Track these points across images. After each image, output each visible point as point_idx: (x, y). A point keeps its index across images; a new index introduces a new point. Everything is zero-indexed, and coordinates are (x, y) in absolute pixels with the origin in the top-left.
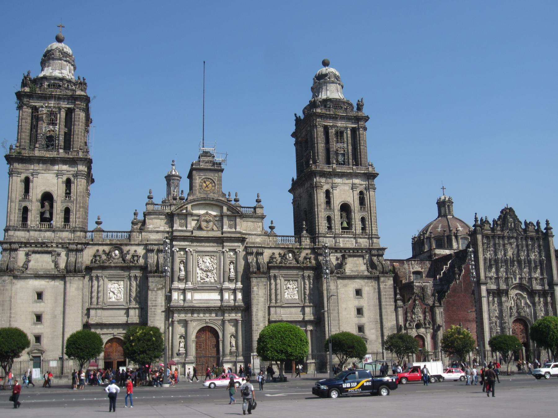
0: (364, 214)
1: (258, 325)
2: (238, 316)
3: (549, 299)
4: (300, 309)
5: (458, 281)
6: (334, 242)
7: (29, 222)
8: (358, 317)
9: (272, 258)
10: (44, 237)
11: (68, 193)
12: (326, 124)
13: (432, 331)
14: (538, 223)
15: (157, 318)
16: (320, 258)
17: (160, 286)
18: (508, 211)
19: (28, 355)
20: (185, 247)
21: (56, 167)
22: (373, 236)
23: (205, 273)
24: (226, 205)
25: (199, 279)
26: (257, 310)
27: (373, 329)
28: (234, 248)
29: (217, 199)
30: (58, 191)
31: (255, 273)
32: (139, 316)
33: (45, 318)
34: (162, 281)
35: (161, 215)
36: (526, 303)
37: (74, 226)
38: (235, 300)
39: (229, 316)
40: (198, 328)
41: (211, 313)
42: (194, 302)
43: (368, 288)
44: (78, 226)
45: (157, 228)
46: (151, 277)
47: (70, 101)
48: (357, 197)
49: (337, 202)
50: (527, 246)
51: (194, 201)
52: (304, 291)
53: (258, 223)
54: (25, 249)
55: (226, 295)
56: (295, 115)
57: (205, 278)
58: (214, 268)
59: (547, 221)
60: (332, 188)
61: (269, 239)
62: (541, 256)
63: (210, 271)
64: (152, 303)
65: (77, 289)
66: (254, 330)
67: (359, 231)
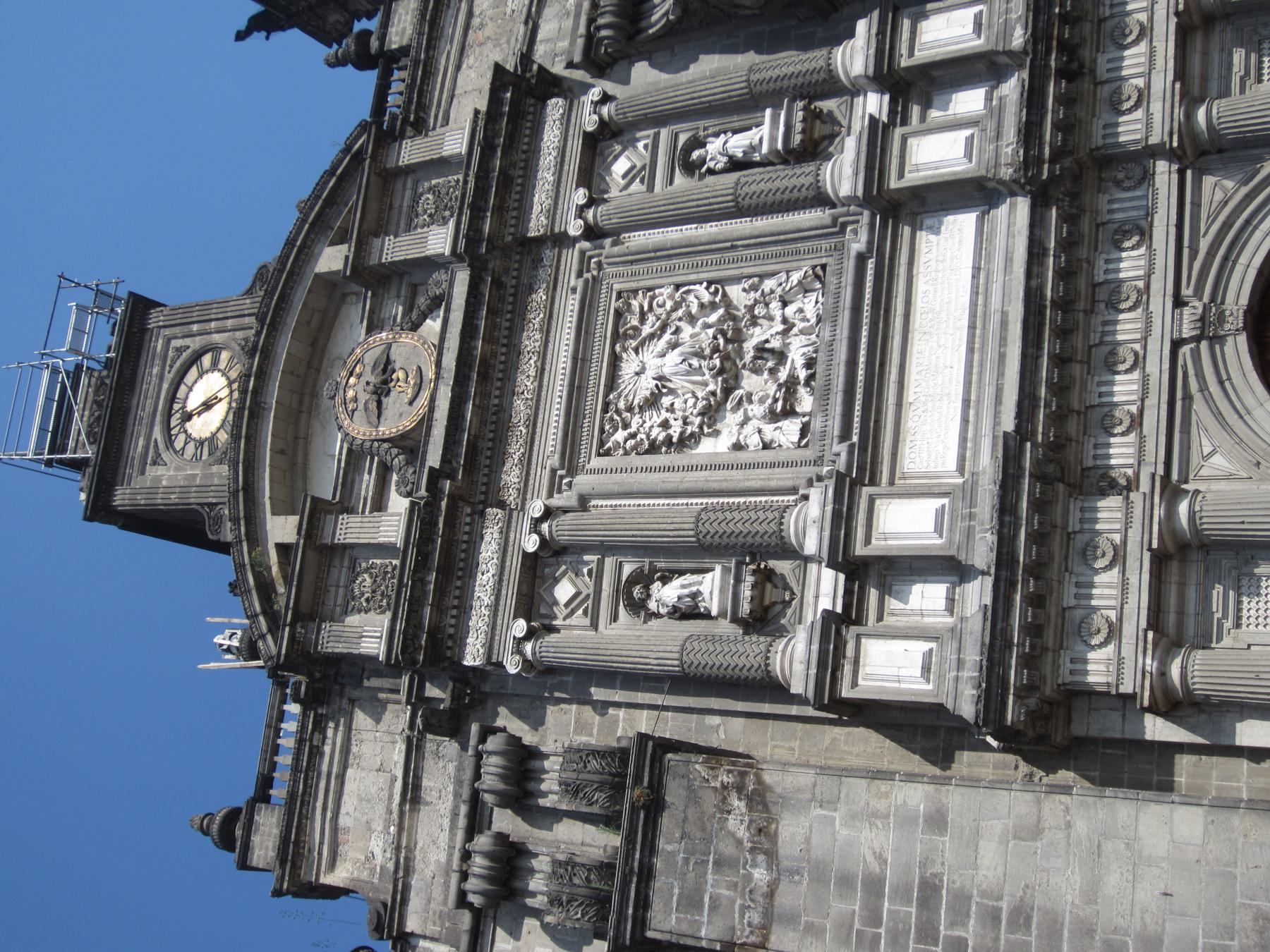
17: (738, 823)
20: (515, 563)
23: (750, 382)
25: (790, 430)
28: (575, 146)
34: (693, 796)
35: (316, 752)
39: (1143, 97)
45: (391, 797)
46: (643, 904)
53: (476, 21)
57: (783, 375)
58: (713, 306)
63: (737, 338)
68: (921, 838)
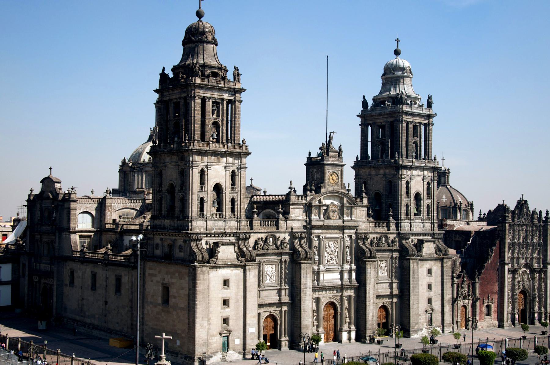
0: (429, 202)
1: (369, 301)
2: (351, 293)
3: (543, 275)
4: (388, 284)
5: (490, 261)
6: (410, 227)
7: (205, 213)
8: (429, 291)
9: (372, 242)
10: (217, 226)
11: (233, 184)
12: (408, 120)
13: (472, 301)
14: (540, 212)
15: (307, 298)
16: (404, 242)
18: (524, 202)
19: (220, 335)
20: (319, 235)
21: (224, 159)
22: (435, 222)
23: (330, 256)
24: (346, 197)
25: (326, 262)
26: (369, 288)
27: (437, 301)
28: (351, 235)
29: (342, 192)
30: (226, 184)
31: (369, 258)
32: (288, 295)
33: (231, 302)
35: (301, 205)
36: (528, 278)
37: (239, 215)
38: (350, 278)
40: (325, 303)
41: (333, 290)
42: (325, 281)
43: (436, 267)
44: (242, 216)
47: (231, 93)
48: (425, 186)
49: (413, 192)
50: (533, 231)
51: (326, 193)
52: (391, 269)
54: (206, 238)
55: (346, 276)
56: (364, 97)
59: (547, 212)
60: (411, 179)
61: (370, 225)
62: (539, 240)
64: (303, 286)
65: (254, 276)
66: (367, 305)
67: (425, 217)
68: (309, 287)
